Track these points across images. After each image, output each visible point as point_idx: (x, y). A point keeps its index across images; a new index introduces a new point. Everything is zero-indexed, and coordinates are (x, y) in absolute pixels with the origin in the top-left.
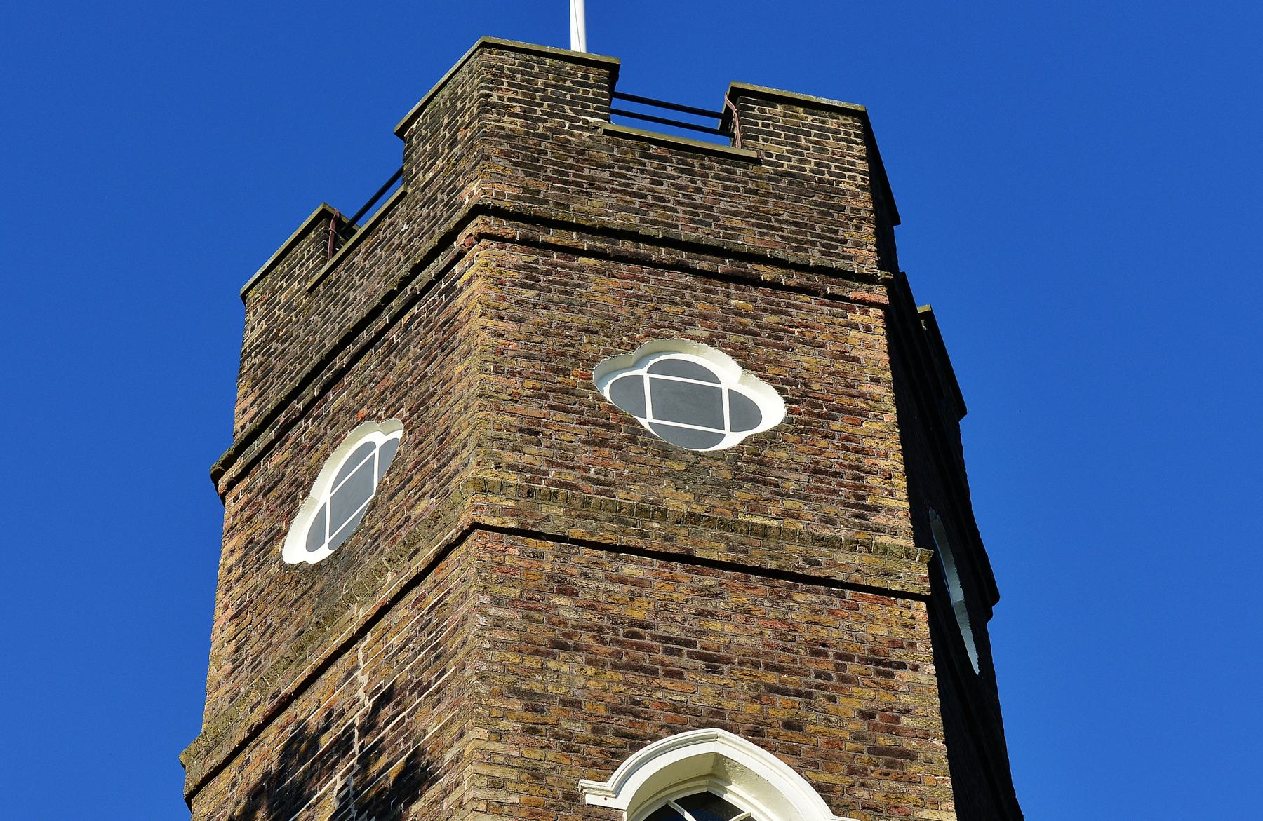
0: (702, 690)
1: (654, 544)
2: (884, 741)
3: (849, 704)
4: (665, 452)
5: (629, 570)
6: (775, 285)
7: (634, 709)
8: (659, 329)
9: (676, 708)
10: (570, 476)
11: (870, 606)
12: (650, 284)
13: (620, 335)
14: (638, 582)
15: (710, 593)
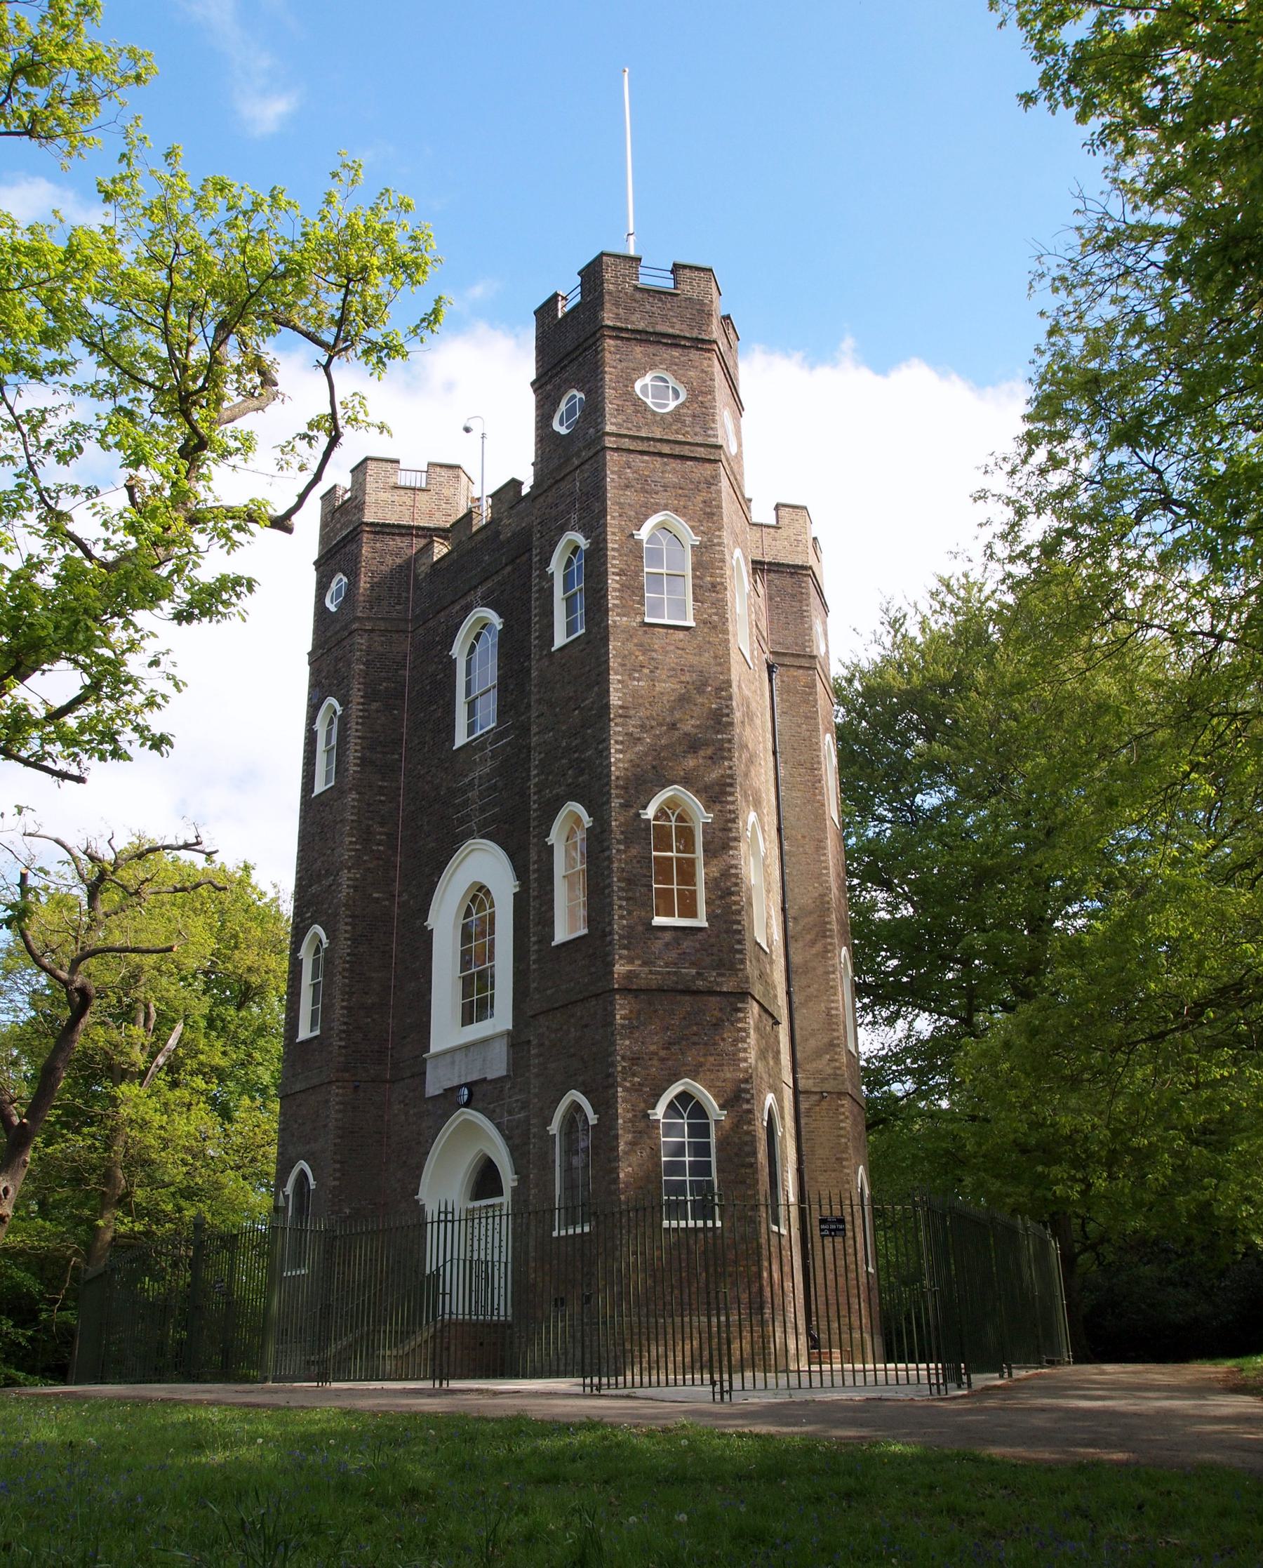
0: (661, 498)
1: (652, 449)
2: (708, 510)
3: (699, 499)
4: (654, 413)
5: (646, 458)
6: (684, 346)
7: (645, 505)
8: (653, 366)
9: (657, 504)
10: (630, 425)
11: (707, 465)
12: (651, 349)
13: (641, 370)
14: (647, 462)
15: (666, 464)
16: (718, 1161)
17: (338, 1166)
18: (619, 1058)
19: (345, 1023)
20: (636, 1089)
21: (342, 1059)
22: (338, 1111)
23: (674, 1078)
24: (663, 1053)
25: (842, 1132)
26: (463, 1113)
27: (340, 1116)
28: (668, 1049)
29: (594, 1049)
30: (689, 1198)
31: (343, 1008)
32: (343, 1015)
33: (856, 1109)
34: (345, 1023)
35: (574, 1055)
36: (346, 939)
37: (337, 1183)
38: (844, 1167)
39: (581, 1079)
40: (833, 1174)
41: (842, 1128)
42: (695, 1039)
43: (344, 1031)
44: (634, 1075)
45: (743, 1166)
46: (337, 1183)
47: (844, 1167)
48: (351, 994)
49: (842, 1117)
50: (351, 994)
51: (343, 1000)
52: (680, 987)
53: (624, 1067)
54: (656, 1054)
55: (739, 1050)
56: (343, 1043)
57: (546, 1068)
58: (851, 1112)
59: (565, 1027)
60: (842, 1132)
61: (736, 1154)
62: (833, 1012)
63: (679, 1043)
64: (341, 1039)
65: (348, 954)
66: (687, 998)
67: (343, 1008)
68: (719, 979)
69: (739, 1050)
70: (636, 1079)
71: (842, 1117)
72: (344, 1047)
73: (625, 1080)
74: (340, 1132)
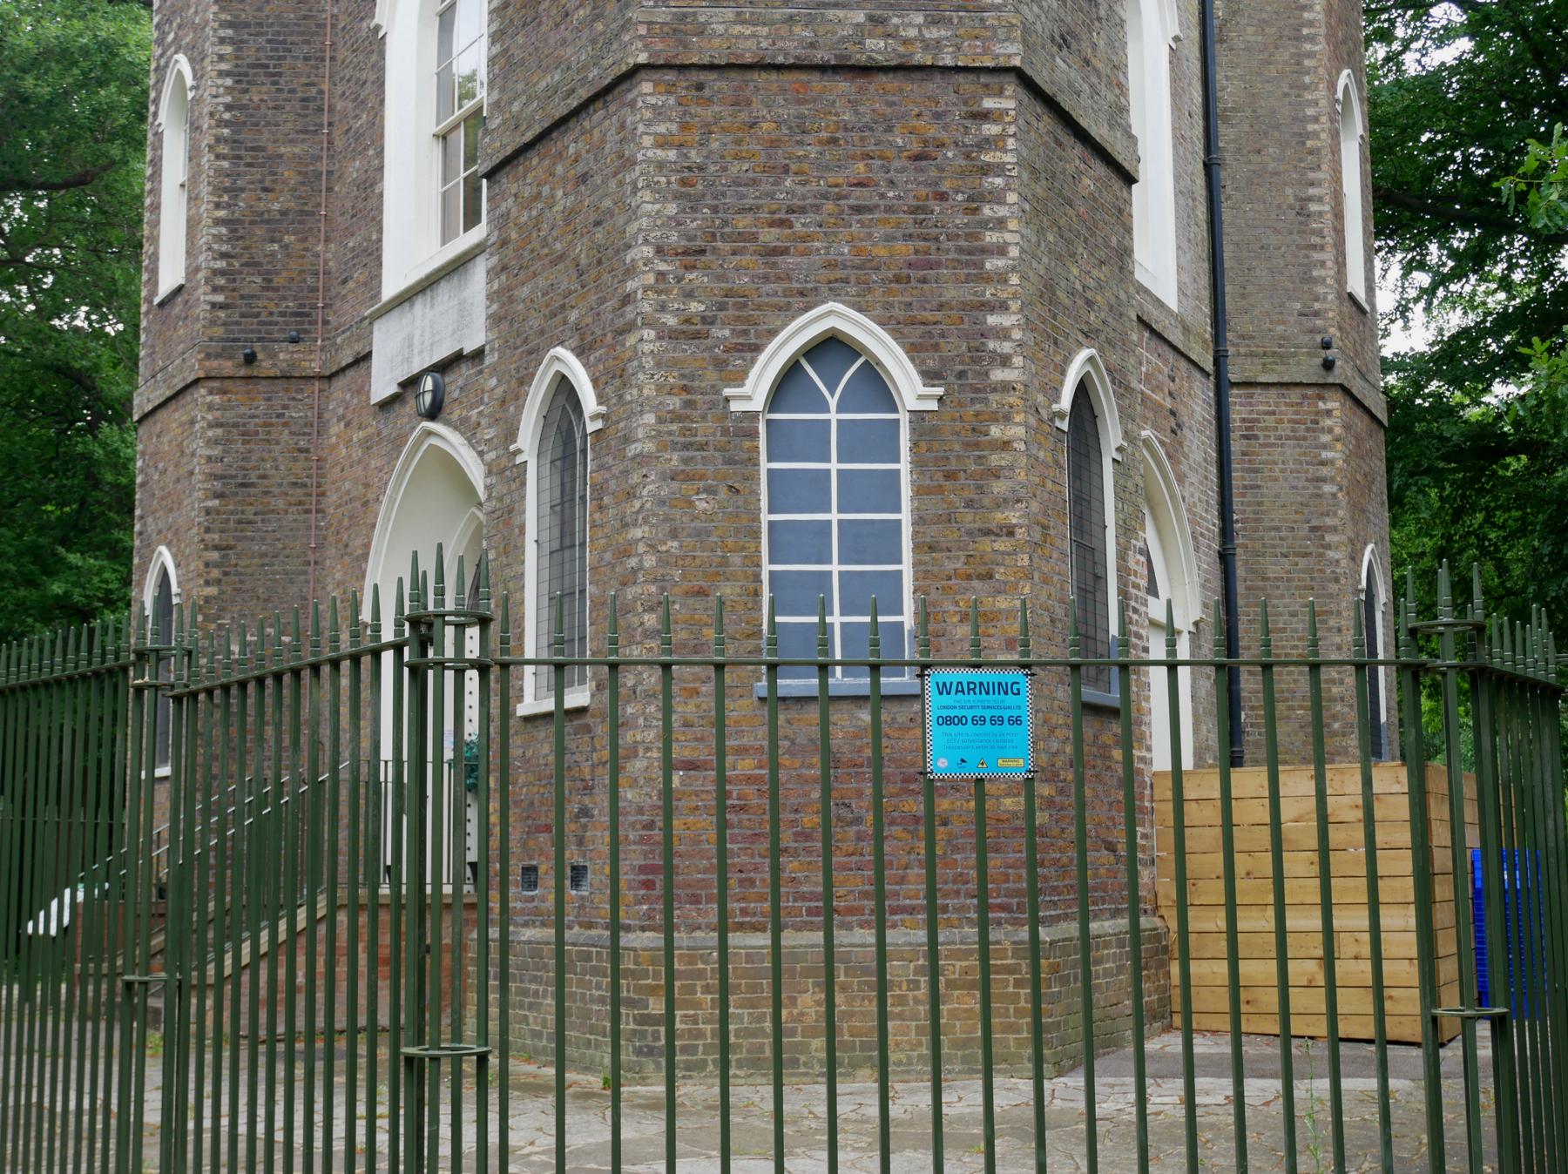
16: (919, 521)
17: (215, 555)
18: (648, 251)
19: (224, 255)
20: (692, 331)
21: (218, 331)
22: (210, 443)
23: (807, 298)
24: (769, 236)
25: (1325, 471)
26: (430, 433)
27: (216, 451)
28: (783, 223)
29: (599, 234)
30: (836, 619)
31: (218, 222)
32: (218, 238)
33: (1361, 423)
34: (224, 255)
35: (562, 257)
36: (221, 74)
37: (212, 591)
38: (1328, 547)
39: (573, 316)
40: (1302, 563)
41: (1323, 463)
42: (859, 196)
43: (222, 273)
44: (689, 295)
45: (987, 533)
46: (212, 591)
47: (1328, 547)
48: (234, 191)
49: (1325, 438)
50: (234, 191)
51: (218, 206)
52: (820, 56)
53: (661, 275)
54: (753, 237)
55: (984, 224)
56: (220, 298)
57: (511, 300)
58: (1347, 427)
59: (546, 190)
60: (1325, 471)
61: (969, 504)
62: (1314, 207)
63: (817, 208)
64: (215, 290)
65: (228, 107)
66: (843, 86)
67: (218, 222)
68: (933, 33)
69: (984, 224)
70: (695, 307)
71: (1325, 438)
72: (222, 306)
73: (663, 308)
74: (218, 485)
